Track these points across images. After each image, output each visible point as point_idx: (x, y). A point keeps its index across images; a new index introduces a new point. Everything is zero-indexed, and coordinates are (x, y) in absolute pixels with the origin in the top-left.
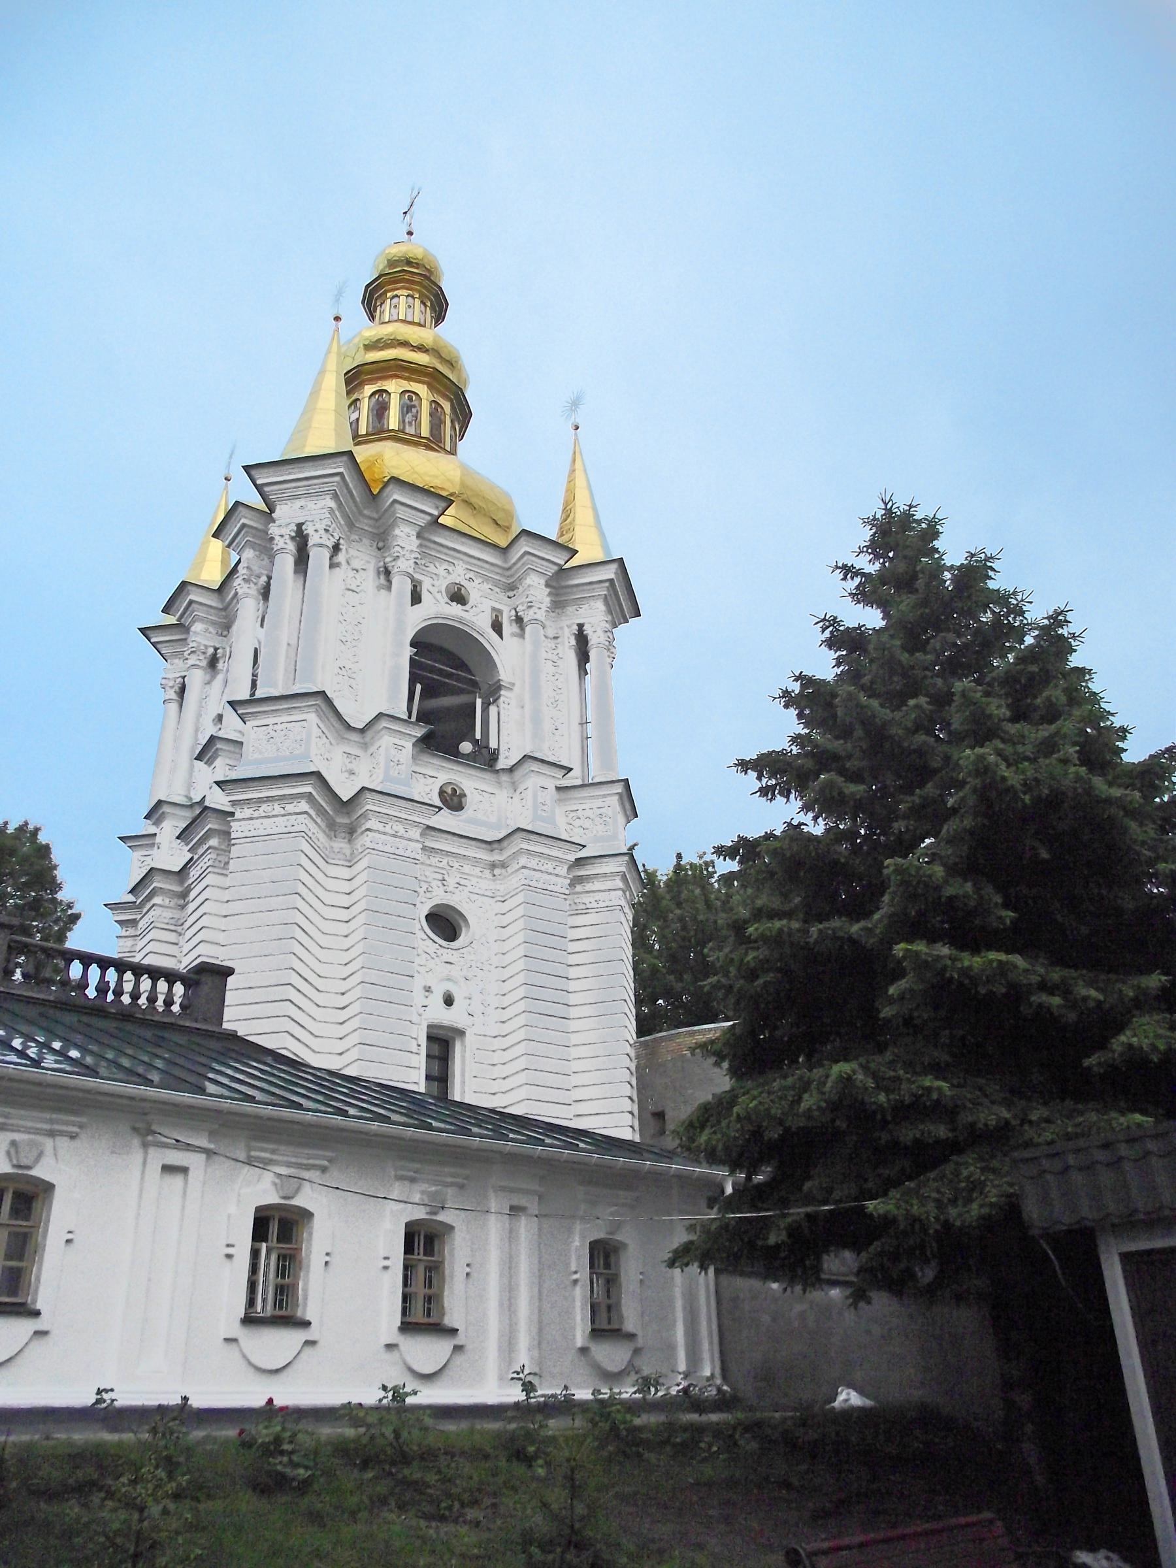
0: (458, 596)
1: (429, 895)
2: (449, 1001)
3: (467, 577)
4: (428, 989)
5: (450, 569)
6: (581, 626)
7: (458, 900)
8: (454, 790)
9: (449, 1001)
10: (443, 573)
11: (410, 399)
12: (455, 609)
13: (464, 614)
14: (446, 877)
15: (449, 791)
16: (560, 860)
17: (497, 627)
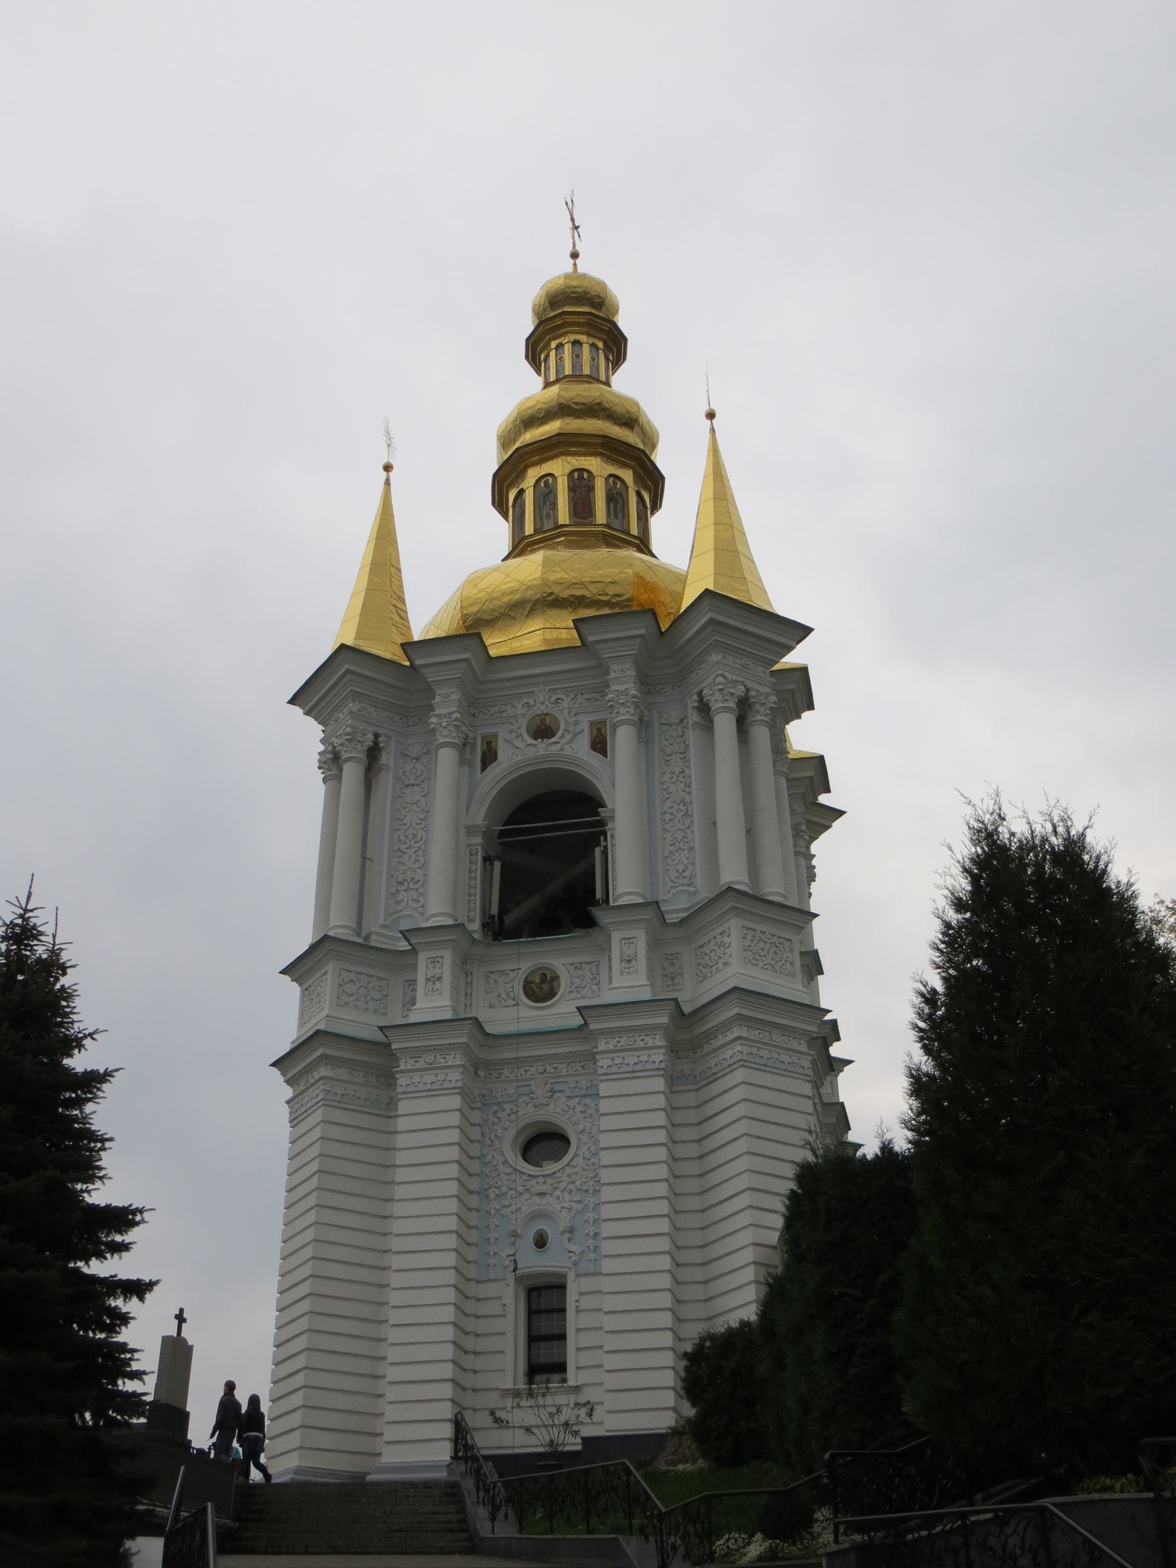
0: (543, 730)
1: (513, 1117)
2: (541, 1242)
3: (553, 699)
4: (514, 1234)
5: (532, 702)
6: (700, 694)
7: (529, 1114)
8: (544, 975)
9: (541, 1242)
10: (521, 711)
11: (546, 483)
12: (542, 747)
13: (554, 749)
14: (533, 1087)
15: (538, 980)
16: (650, 1029)
17: (600, 745)
